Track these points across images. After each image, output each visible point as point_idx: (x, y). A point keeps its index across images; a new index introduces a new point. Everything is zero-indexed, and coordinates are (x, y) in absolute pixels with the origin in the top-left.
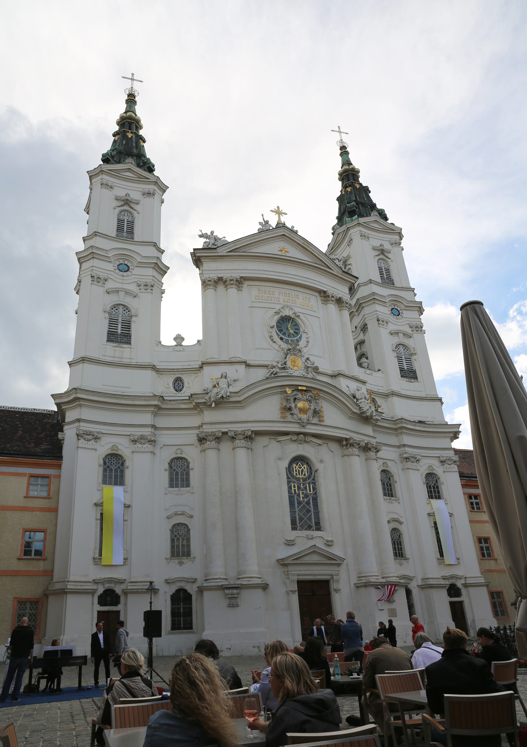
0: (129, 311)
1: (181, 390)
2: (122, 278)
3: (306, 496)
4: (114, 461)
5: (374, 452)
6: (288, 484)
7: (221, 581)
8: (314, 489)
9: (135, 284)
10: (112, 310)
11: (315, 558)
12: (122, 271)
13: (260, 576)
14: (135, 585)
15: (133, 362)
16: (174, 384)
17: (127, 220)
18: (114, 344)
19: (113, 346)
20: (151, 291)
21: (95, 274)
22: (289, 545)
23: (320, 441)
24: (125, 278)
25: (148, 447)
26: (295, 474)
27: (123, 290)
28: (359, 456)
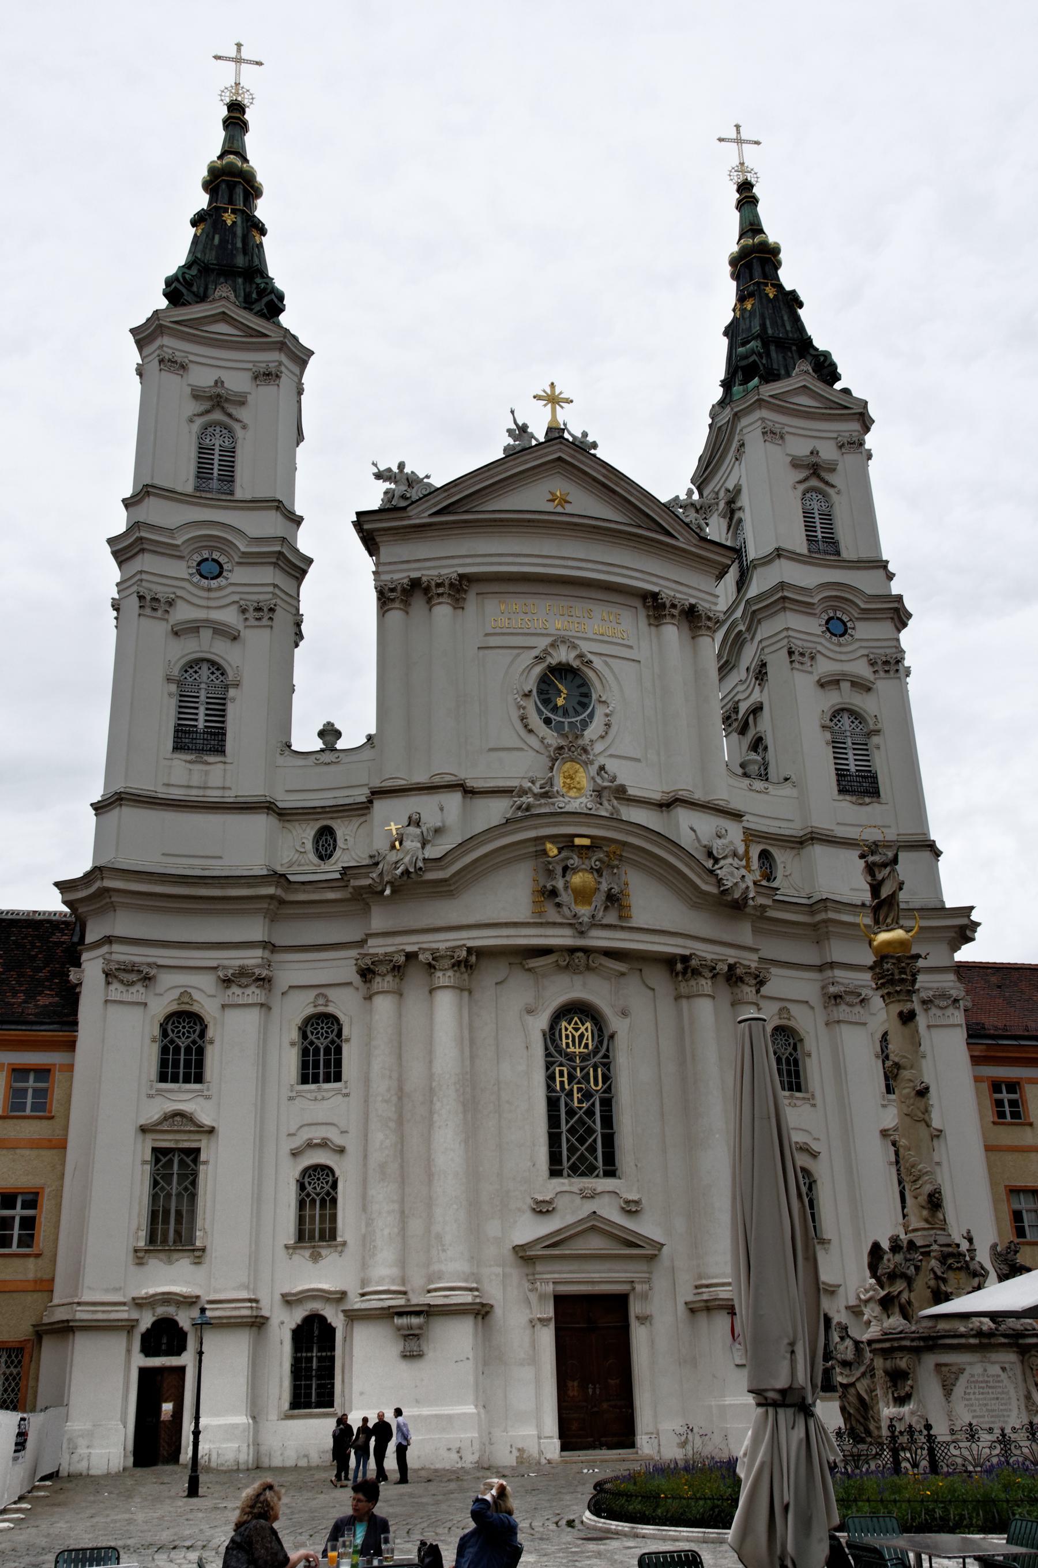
0: (222, 674)
1: (331, 856)
2: (205, 594)
3: (587, 1095)
4: (184, 1027)
5: (750, 986)
6: (547, 1069)
8: (606, 1078)
9: (235, 607)
10: (186, 675)
11: (595, 1244)
12: (206, 578)
13: (474, 1285)
14: (217, 1309)
15: (230, 796)
16: (318, 842)
17: (220, 446)
18: (189, 757)
19: (186, 761)
20: (269, 623)
21: (145, 591)
22: (541, 1212)
23: (623, 964)
24: (213, 595)
25: (253, 994)
26: (564, 1046)
27: (208, 623)
28: (714, 998)
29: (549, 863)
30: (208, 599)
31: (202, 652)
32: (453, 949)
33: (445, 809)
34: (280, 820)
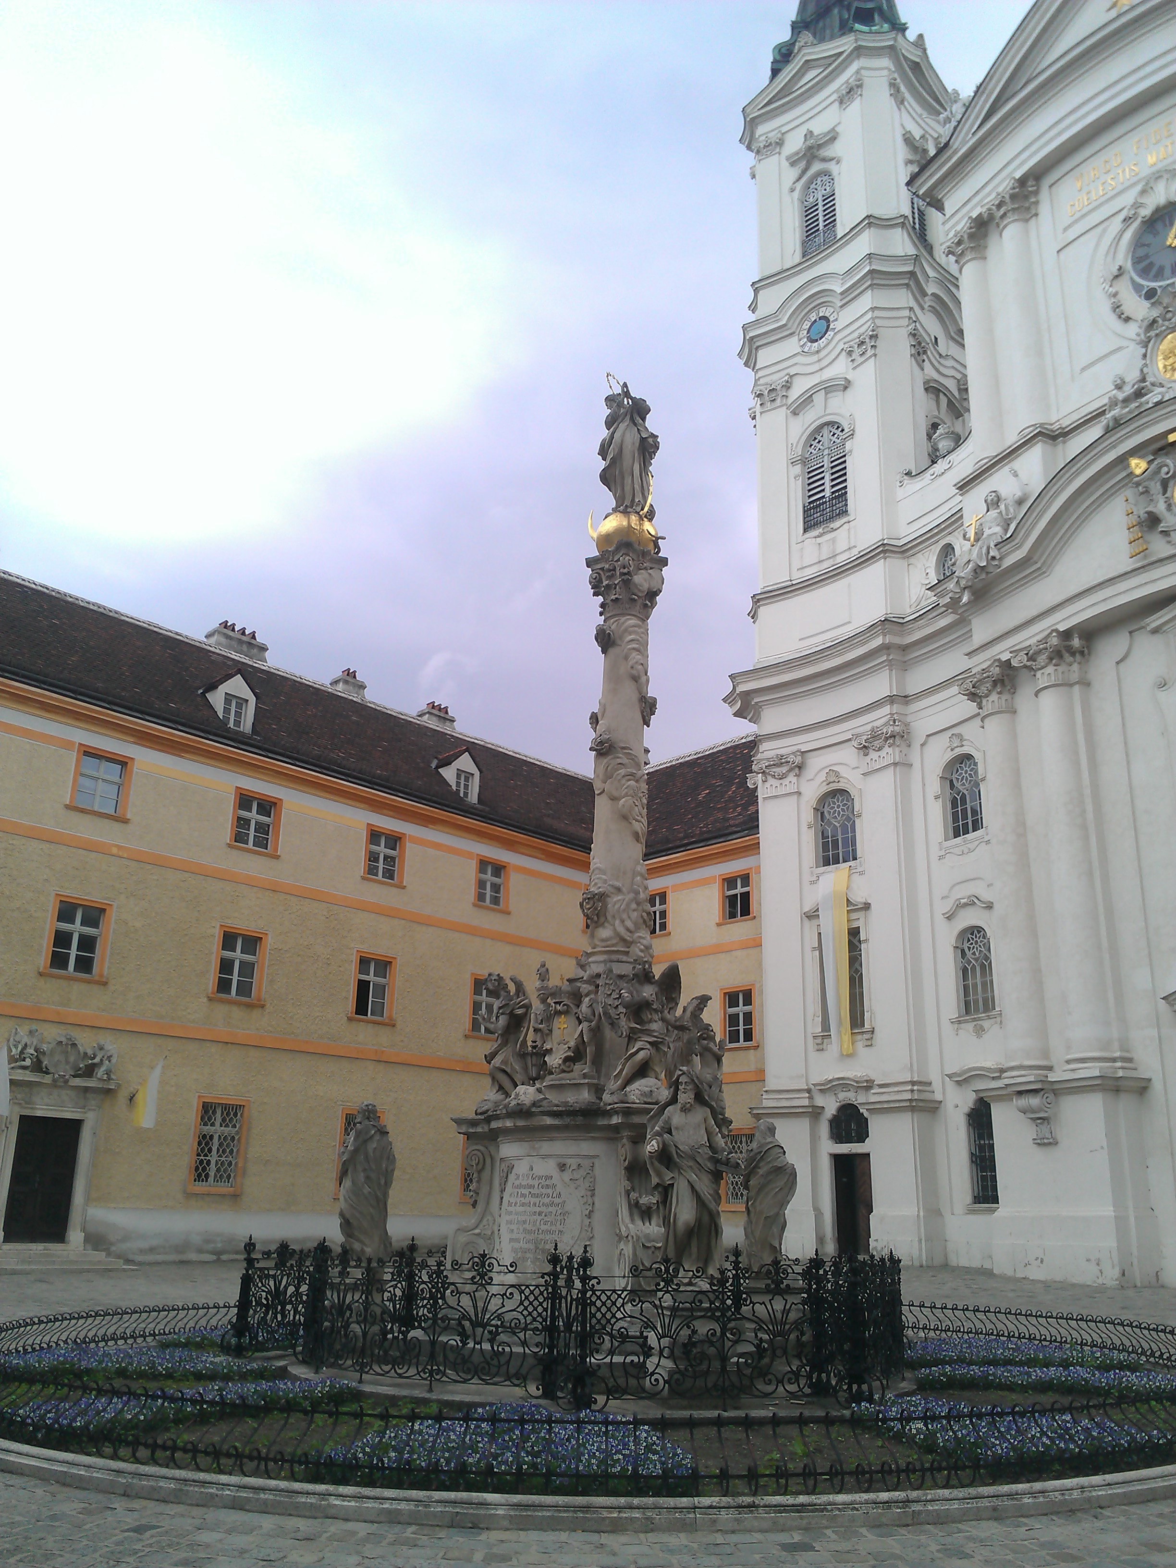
2: (815, 358)
4: (838, 806)
7: (1023, 1073)
9: (844, 353)
10: (811, 450)
12: (817, 341)
24: (823, 354)
25: (889, 754)
29: (1138, 484)
30: (819, 360)
31: (819, 418)
32: (1045, 640)
33: (1019, 473)
34: (904, 558)
